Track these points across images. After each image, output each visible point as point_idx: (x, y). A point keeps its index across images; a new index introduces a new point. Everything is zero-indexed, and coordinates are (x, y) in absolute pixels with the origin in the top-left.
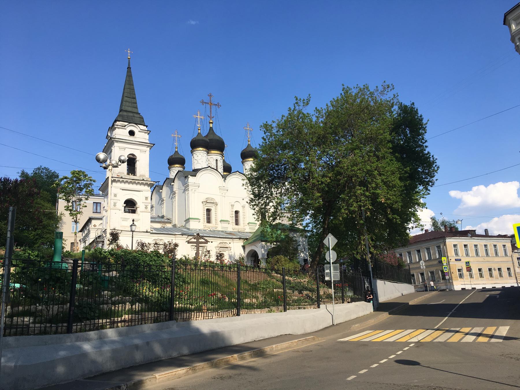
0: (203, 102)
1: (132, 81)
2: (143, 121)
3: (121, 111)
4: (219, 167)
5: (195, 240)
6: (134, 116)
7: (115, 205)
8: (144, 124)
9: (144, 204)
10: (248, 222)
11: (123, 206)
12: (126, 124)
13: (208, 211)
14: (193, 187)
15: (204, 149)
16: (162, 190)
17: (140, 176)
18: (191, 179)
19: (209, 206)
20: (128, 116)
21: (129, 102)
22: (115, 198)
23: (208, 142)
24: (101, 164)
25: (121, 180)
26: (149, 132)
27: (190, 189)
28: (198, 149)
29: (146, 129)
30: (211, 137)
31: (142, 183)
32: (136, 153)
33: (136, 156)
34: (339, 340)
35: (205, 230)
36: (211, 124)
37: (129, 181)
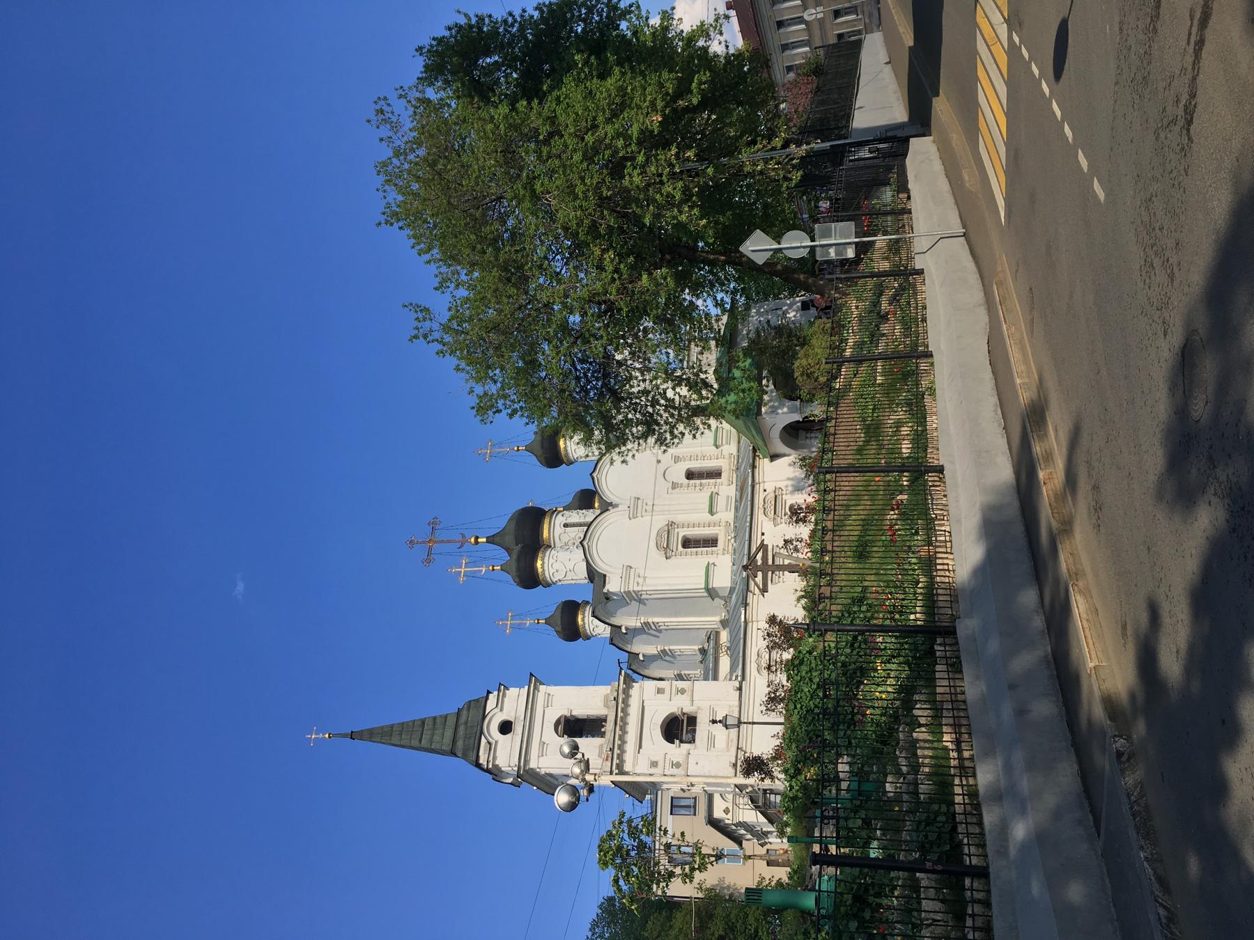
0: (428, 560)
1: (383, 727)
2: (477, 700)
3: (453, 754)
4: (582, 520)
5: (760, 574)
6: (466, 723)
7: (678, 765)
8: (484, 700)
9: (673, 696)
10: (714, 447)
11: (680, 746)
12: (483, 741)
13: (687, 543)
14: (632, 580)
15: (540, 555)
16: (638, 655)
17: (606, 705)
18: (613, 586)
19: (676, 543)
20: (466, 737)
21: (433, 735)
22: (661, 764)
23: (522, 548)
24: (583, 798)
25: (616, 751)
26: (502, 687)
27: (636, 589)
28: (540, 570)
29: (496, 693)
30: (509, 539)
31: (623, 702)
32: (554, 714)
33: (560, 717)
34: (1003, 220)
35: (735, 550)
36: (479, 540)
37: (618, 732)
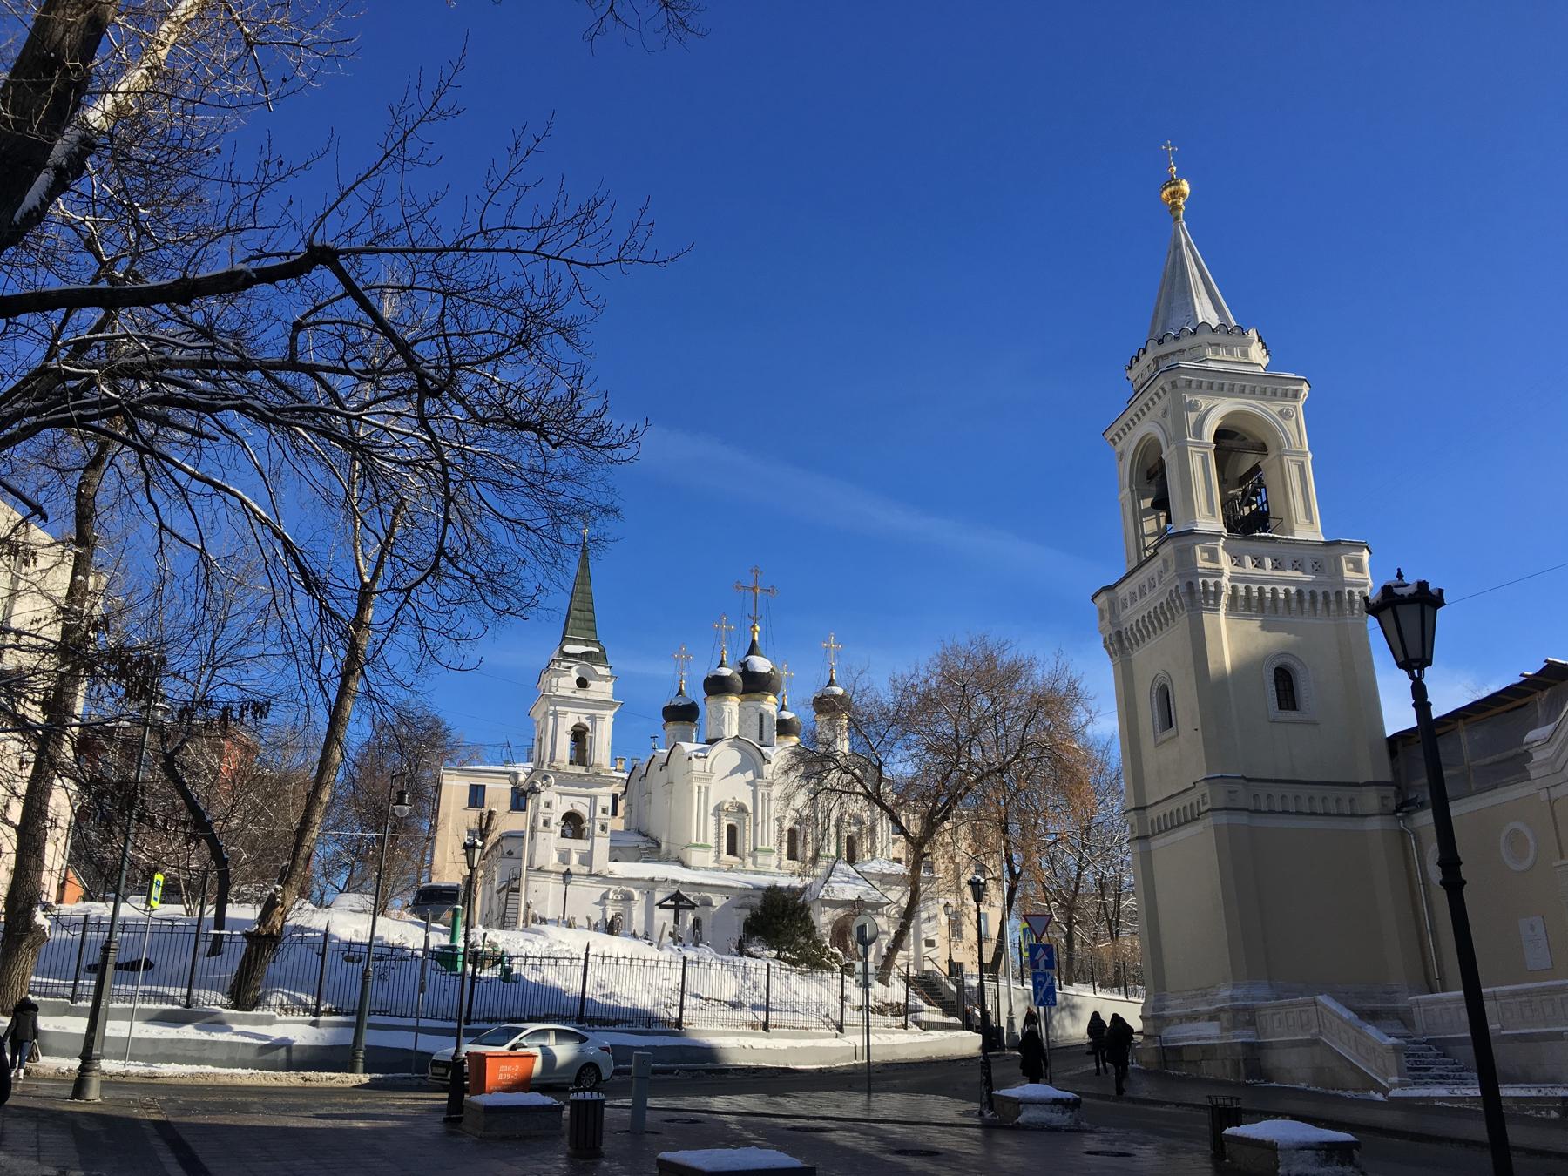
0: (739, 586)
5: (673, 903)
21: (580, 620)
22: (548, 810)
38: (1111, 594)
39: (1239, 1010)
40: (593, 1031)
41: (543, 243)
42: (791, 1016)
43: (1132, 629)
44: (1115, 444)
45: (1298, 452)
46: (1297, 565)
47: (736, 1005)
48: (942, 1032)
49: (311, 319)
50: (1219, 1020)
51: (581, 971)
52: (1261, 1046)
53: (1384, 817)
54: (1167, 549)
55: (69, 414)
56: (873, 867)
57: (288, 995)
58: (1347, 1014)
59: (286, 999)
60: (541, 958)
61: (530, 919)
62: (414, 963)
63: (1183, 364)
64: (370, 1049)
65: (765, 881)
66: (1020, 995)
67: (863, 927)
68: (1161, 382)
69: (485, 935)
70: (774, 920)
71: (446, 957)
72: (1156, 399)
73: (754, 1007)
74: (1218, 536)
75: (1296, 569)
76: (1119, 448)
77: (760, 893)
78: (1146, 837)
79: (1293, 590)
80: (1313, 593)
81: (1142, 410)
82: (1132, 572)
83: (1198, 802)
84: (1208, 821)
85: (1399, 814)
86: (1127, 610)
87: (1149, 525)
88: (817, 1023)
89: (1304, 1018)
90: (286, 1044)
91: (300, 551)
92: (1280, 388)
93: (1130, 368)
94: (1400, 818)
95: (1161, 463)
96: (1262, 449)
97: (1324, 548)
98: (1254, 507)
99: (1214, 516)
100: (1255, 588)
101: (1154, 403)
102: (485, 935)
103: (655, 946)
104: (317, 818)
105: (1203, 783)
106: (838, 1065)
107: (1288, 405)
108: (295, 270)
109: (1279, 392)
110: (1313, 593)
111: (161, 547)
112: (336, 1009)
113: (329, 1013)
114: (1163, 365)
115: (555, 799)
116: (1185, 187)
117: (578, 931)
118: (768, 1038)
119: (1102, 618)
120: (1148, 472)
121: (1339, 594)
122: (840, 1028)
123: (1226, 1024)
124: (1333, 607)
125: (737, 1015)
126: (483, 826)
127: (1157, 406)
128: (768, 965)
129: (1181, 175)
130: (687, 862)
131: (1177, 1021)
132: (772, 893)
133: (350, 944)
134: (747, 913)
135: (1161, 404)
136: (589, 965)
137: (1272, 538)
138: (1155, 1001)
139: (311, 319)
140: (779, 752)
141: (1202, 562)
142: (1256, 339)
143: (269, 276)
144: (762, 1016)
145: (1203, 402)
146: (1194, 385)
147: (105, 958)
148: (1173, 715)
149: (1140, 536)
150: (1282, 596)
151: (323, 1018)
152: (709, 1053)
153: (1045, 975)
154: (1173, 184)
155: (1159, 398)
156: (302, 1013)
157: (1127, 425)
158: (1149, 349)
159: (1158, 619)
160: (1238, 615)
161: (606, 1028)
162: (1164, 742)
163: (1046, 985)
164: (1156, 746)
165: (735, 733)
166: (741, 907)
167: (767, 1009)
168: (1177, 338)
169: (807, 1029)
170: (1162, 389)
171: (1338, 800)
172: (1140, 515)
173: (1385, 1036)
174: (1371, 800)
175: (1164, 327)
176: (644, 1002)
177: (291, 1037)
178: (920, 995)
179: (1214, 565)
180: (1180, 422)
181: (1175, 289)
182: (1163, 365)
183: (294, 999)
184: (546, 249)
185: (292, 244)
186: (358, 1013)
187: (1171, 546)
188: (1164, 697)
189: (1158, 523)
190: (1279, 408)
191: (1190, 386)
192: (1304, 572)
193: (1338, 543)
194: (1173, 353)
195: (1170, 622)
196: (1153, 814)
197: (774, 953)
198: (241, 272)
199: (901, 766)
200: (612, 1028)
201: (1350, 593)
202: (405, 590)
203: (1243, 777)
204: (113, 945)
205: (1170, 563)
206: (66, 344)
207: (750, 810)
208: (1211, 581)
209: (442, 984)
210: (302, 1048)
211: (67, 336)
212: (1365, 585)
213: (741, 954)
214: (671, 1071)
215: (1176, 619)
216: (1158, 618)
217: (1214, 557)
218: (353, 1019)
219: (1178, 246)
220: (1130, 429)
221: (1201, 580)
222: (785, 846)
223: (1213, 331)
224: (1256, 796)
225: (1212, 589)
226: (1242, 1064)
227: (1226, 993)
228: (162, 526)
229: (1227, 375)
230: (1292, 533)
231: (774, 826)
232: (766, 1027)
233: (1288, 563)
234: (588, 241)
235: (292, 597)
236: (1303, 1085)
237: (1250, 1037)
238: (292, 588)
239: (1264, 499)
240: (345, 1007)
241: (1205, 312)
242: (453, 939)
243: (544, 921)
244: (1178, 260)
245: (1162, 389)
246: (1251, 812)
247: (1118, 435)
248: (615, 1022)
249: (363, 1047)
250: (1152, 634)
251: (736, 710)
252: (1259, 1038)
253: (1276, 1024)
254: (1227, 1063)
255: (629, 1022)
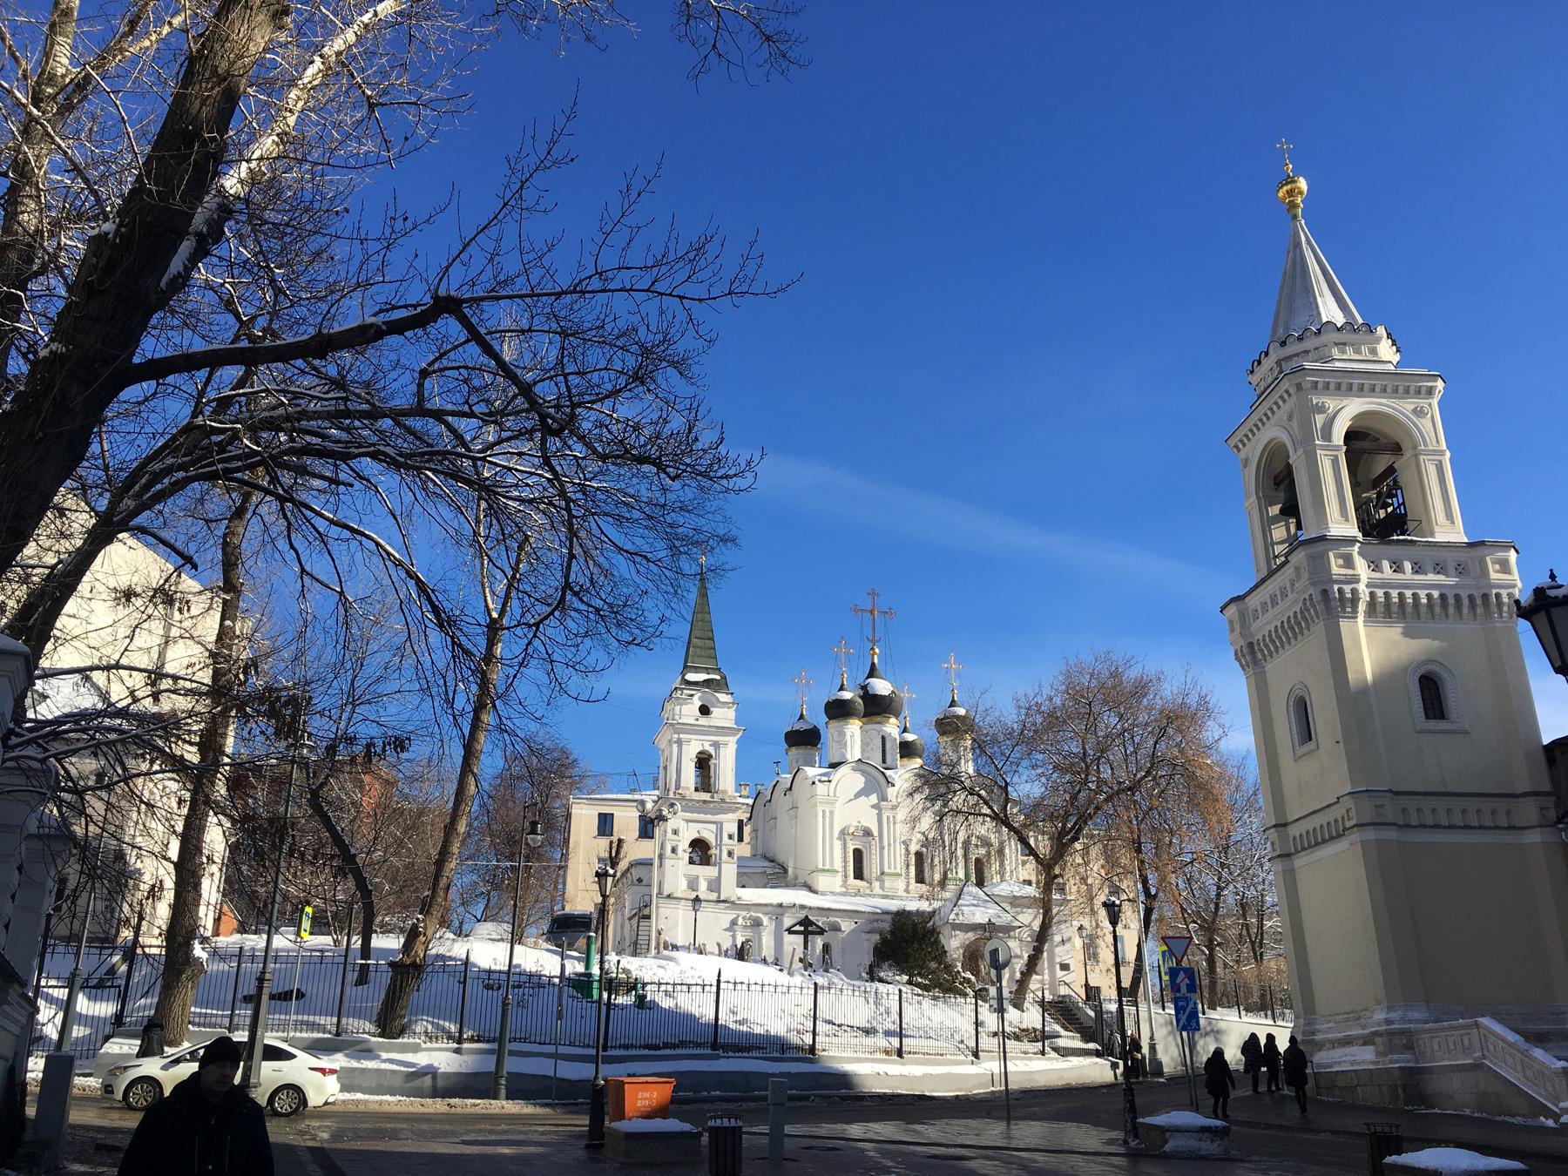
5: (802, 928)
22: (675, 837)
38: (1240, 604)
39: (1395, 1033)
40: (728, 1057)
41: (656, 281)
42: (924, 1042)
43: (1264, 640)
44: (1239, 450)
45: (1435, 451)
46: (1439, 568)
47: (868, 1032)
48: (1081, 1059)
49: (436, 366)
50: (1373, 1043)
51: (714, 997)
52: (1420, 1071)
53: (1544, 830)
54: (1298, 557)
55: (214, 468)
56: (1004, 889)
57: (432, 1023)
58: (1512, 1037)
59: (430, 1027)
60: (674, 984)
61: (662, 945)
62: (551, 989)
63: (1308, 365)
64: (514, 1077)
65: (893, 905)
66: (1161, 1020)
67: (996, 950)
68: (1285, 385)
69: (619, 962)
70: (904, 945)
71: (581, 984)
72: (1281, 403)
73: (888, 1033)
74: (1352, 541)
75: (1438, 573)
76: (1243, 455)
77: (889, 917)
78: (1288, 855)
79: (1436, 594)
80: (1457, 597)
81: (1266, 415)
82: (1263, 581)
83: (1343, 818)
84: (1355, 837)
85: (1561, 826)
86: (1258, 621)
87: (1279, 533)
88: (952, 1049)
89: (1466, 1043)
90: (430, 1071)
91: (433, 590)
92: (1413, 385)
93: (1252, 372)
94: (1562, 830)
95: (1288, 471)
96: (1397, 449)
97: (1468, 549)
98: (1390, 509)
99: (1347, 520)
100: (1394, 593)
101: (1279, 407)
102: (619, 962)
103: (785, 972)
104: (455, 848)
105: (1347, 797)
106: (975, 1092)
107: (1423, 402)
108: (421, 320)
109: (1412, 389)
110: (1457, 597)
111: (303, 591)
112: (478, 1036)
113: (472, 1040)
114: (1287, 368)
115: (682, 826)
116: (1302, 184)
117: (709, 957)
118: (903, 1064)
119: (1232, 630)
120: (1275, 477)
121: (1485, 597)
122: (976, 1055)
123: (1381, 1048)
124: (1480, 610)
125: (870, 1041)
126: (613, 855)
127: (1282, 410)
128: (900, 991)
129: (1299, 171)
130: (815, 887)
131: (1330, 1046)
132: (901, 917)
133: (489, 972)
134: (877, 937)
135: (1285, 408)
136: (721, 991)
137: (1411, 541)
138: (1305, 1025)
139: (436, 366)
140: (904, 774)
141: (1336, 568)
142: (1385, 335)
143: (398, 328)
144: (895, 1042)
145: (1331, 403)
146: (1320, 386)
147: (260, 989)
148: (1312, 727)
149: (1269, 544)
150: (1424, 601)
151: (466, 1046)
152: (844, 1080)
153: (1187, 1000)
154: (1290, 182)
155: (1284, 401)
156: (445, 1041)
157: (1251, 431)
158: (1271, 352)
159: (1292, 629)
160: (1378, 622)
161: (740, 1054)
162: (1303, 755)
163: (1189, 1009)
164: (1295, 761)
165: (858, 756)
166: (870, 932)
167: (901, 1036)
168: (1300, 338)
169: (942, 1055)
170: (1287, 392)
171: (1493, 812)
172: (1267, 523)
173: (1555, 1060)
174: (1529, 811)
175: (1287, 328)
176: (777, 1028)
177: (436, 1064)
178: (1057, 1021)
179: (1350, 572)
180: (1307, 426)
181: (1297, 287)
182: (1287, 368)
183: (437, 1026)
184: (659, 287)
185: (418, 295)
186: (498, 1041)
187: (1303, 553)
188: (1302, 709)
189: (1288, 530)
190: (1413, 407)
191: (1316, 388)
192: (1447, 575)
193: (1482, 543)
194: (1297, 355)
195: (1305, 632)
196: (1294, 830)
197: (905, 978)
198: (372, 325)
199: (1028, 786)
200: (746, 1054)
201: (1498, 596)
202: (534, 625)
203: (1391, 791)
204: (267, 976)
205: (1302, 571)
206: (210, 401)
207: (876, 833)
208: (1347, 588)
209: (579, 1011)
210: (447, 1075)
211: (212, 394)
212: (1514, 586)
213: (872, 979)
214: (806, 1098)
215: (1312, 628)
216: (1292, 628)
217: (1348, 562)
218: (495, 1046)
219: (1298, 245)
220: (1254, 434)
221: (1336, 587)
222: (912, 869)
223: (1338, 329)
224: (1404, 810)
225: (1349, 596)
226: (1400, 1090)
227: (1380, 1016)
228: (303, 570)
229: (1356, 375)
230: (1432, 534)
231: (901, 850)
232: (900, 1053)
233: (1429, 566)
234: (700, 276)
235: (426, 635)
236: (1467, 1112)
237: (1408, 1061)
238: (426, 626)
239: (1401, 501)
240: (487, 1035)
241: (1329, 310)
242: (587, 966)
243: (675, 947)
244: (1298, 258)
245: (1287, 392)
246: (1400, 826)
247: (1241, 441)
248: (749, 1049)
249: (505, 1073)
250: (1286, 644)
251: (858, 733)
252: (1417, 1061)
253: (1436, 1047)
254: (1384, 1088)
255: (763, 1048)
